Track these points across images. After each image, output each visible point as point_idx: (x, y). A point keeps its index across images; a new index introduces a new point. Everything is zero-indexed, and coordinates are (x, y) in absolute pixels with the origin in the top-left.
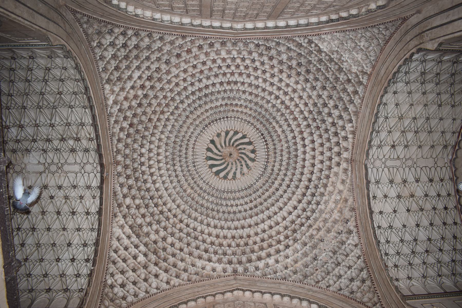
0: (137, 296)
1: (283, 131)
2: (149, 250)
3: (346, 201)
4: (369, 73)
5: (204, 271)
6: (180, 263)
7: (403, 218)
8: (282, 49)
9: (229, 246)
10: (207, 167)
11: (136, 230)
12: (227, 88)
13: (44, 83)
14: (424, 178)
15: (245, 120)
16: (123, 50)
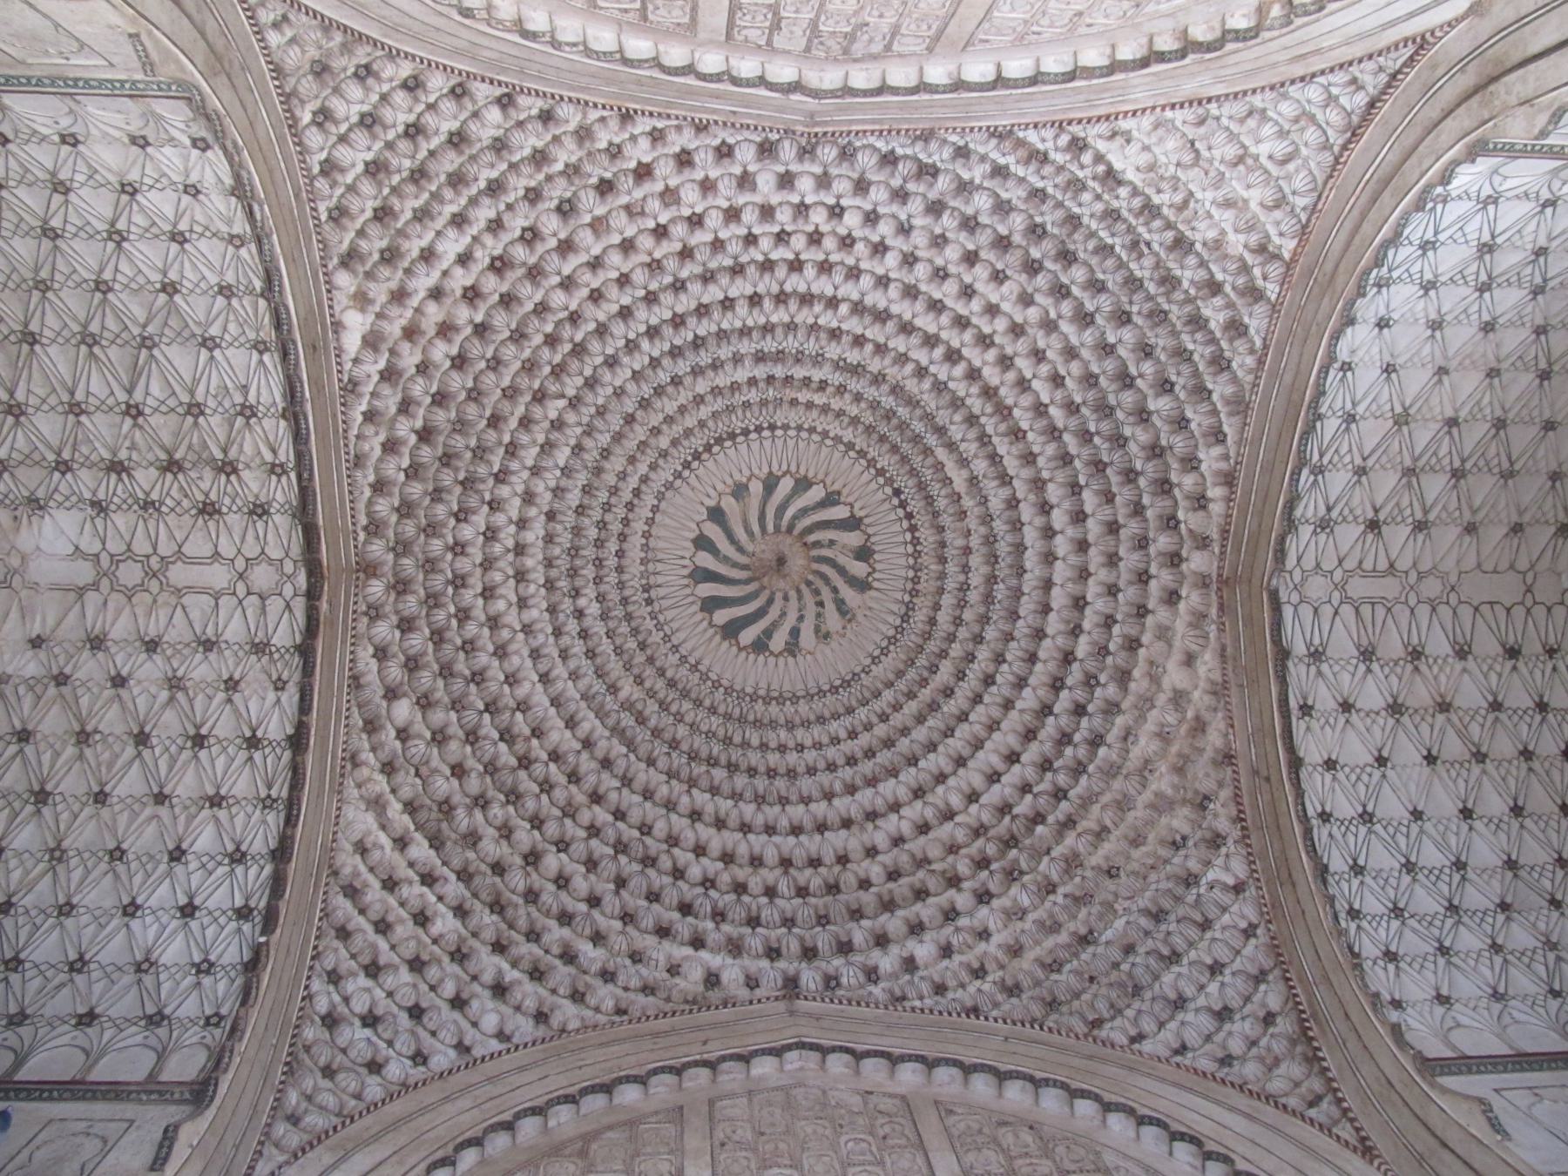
0: (425, 1062)
1: (973, 481)
2: (475, 895)
3: (1200, 726)
4: (1287, 256)
5: (677, 980)
6: (586, 949)
7: (1413, 788)
8: (976, 173)
9: (771, 892)
10: (696, 608)
11: (433, 819)
13: (111, 245)
14: (1486, 644)
15: (838, 439)
16: (404, 145)
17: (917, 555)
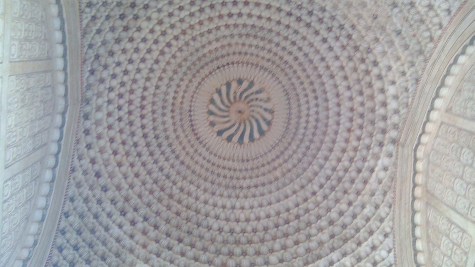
1: (217, 40)
2: (340, 247)
5: (384, 182)
8: (98, 40)
9: (359, 139)
12: (150, 109)
15: (197, 88)
16: (81, 250)
17: (243, 63)
